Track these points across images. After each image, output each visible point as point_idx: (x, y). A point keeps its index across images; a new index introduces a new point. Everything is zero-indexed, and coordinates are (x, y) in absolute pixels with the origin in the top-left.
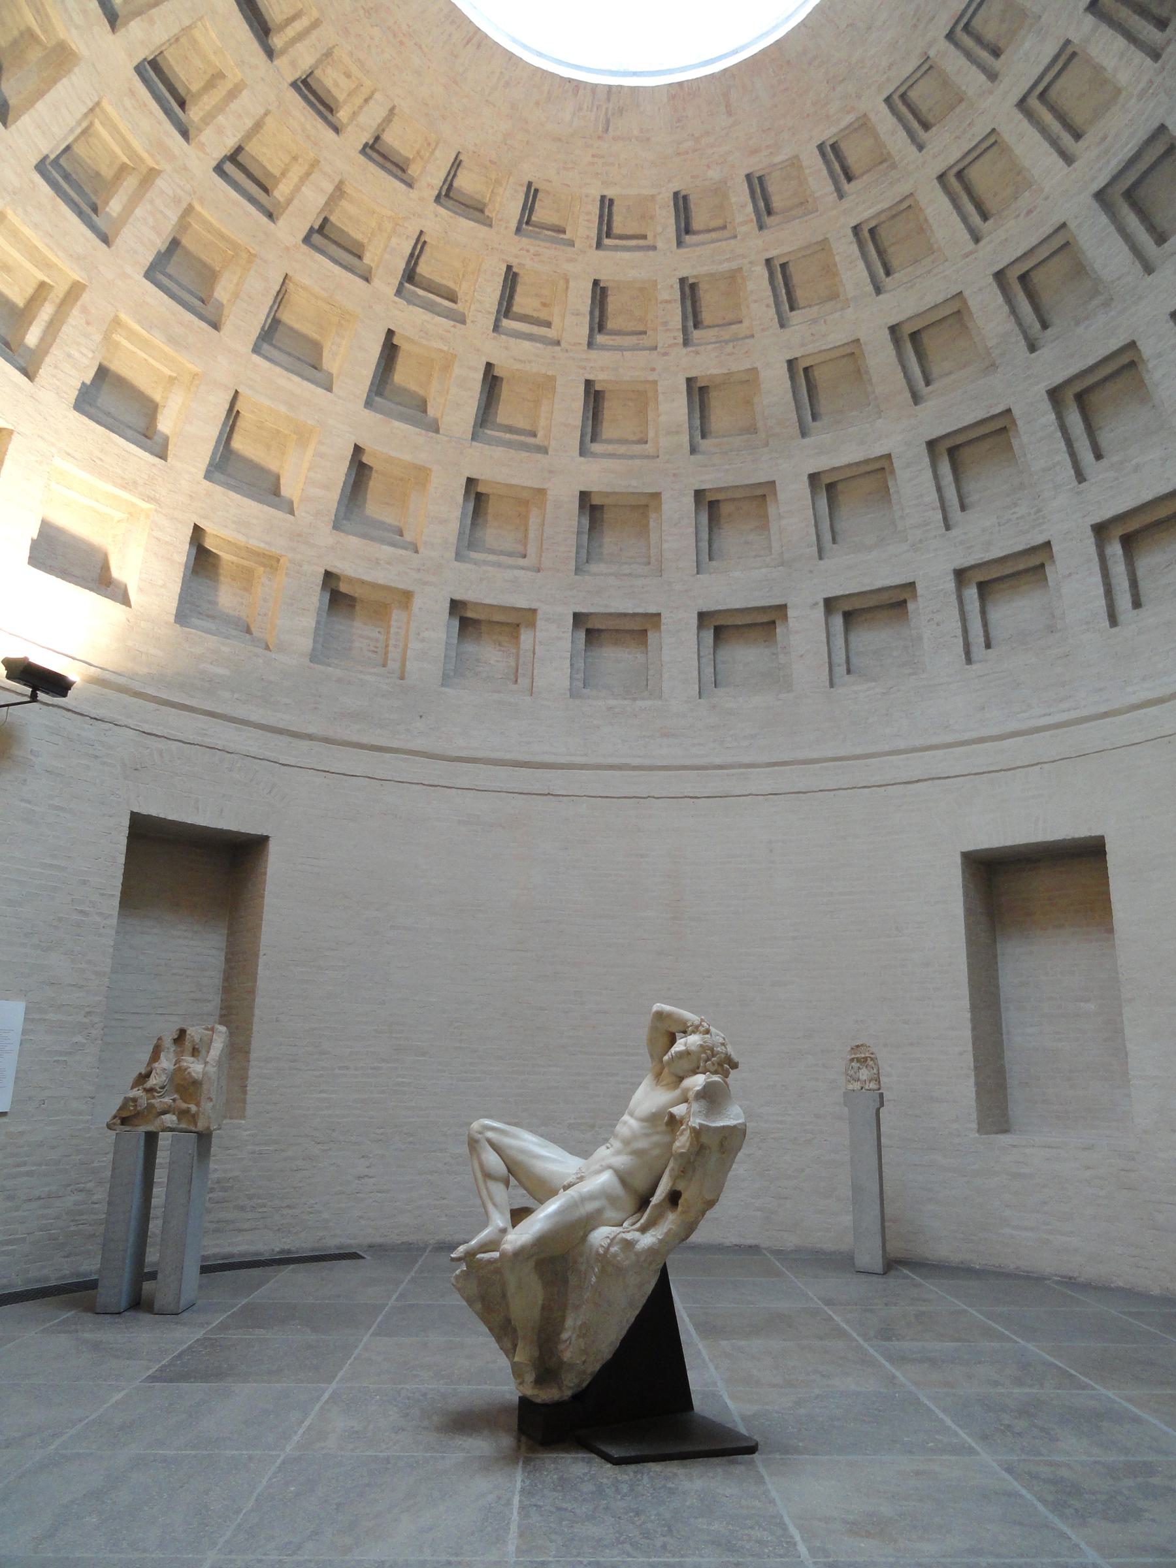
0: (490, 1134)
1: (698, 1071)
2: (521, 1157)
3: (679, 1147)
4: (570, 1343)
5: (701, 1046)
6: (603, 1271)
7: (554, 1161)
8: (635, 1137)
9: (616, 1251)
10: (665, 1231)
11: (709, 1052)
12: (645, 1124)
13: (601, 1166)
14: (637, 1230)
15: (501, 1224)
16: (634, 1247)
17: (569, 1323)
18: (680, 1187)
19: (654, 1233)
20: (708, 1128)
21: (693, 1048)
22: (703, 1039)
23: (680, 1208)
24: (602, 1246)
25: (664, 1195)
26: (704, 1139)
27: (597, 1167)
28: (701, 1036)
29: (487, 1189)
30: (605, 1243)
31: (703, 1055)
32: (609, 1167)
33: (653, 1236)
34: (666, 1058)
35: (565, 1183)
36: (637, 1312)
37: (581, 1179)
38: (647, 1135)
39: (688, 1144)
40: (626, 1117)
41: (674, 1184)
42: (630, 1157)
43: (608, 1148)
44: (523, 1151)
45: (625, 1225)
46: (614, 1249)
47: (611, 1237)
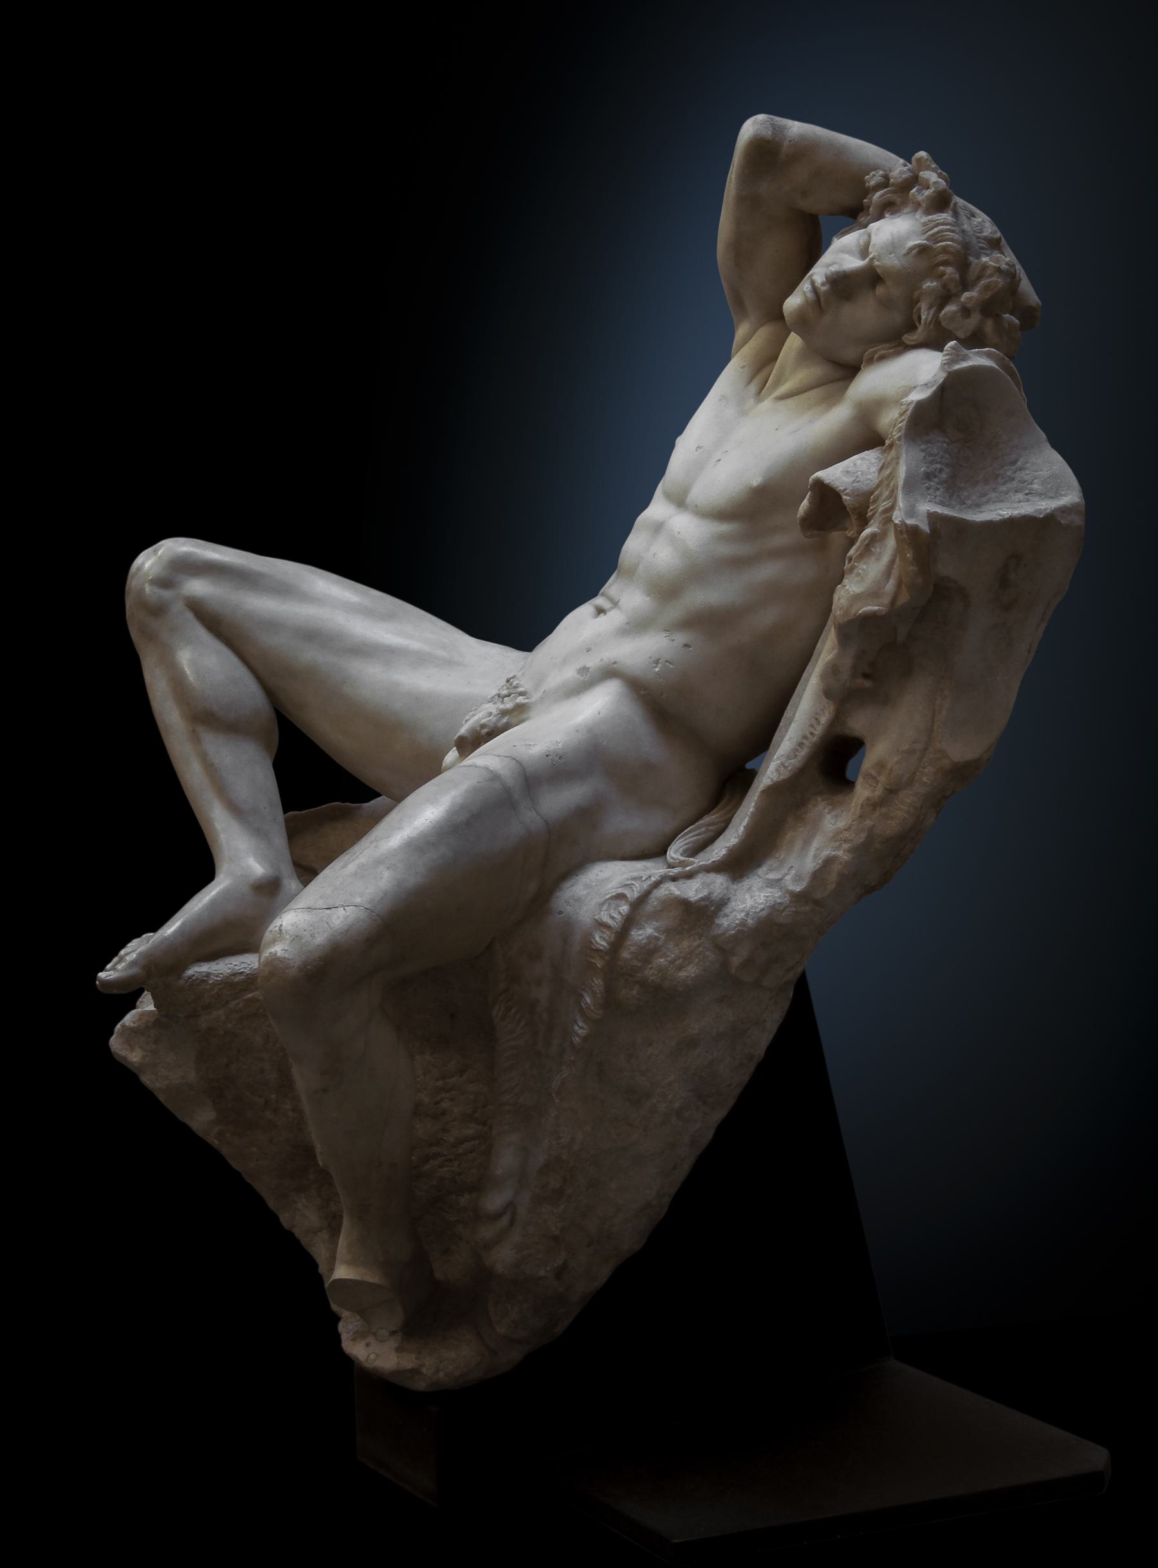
0: (198, 587)
1: (908, 338)
2: (309, 655)
3: (856, 598)
4: (512, 1222)
5: (922, 250)
6: (610, 1001)
7: (420, 660)
9: (649, 937)
11: (949, 270)
13: (584, 670)
14: (717, 868)
15: (257, 869)
16: (713, 923)
17: (505, 1160)
18: (858, 723)
19: (772, 876)
20: (960, 528)
21: (893, 261)
23: (862, 792)
24: (601, 925)
25: (803, 753)
26: (947, 567)
27: (569, 674)
28: (921, 218)
29: (204, 758)
30: (614, 915)
32: (610, 672)
33: (772, 884)
34: (793, 302)
36: (719, 1115)
38: (736, 563)
39: (890, 586)
40: (657, 509)
41: (838, 718)
42: (681, 638)
43: (600, 611)
45: (674, 852)
46: (642, 934)
47: (633, 894)
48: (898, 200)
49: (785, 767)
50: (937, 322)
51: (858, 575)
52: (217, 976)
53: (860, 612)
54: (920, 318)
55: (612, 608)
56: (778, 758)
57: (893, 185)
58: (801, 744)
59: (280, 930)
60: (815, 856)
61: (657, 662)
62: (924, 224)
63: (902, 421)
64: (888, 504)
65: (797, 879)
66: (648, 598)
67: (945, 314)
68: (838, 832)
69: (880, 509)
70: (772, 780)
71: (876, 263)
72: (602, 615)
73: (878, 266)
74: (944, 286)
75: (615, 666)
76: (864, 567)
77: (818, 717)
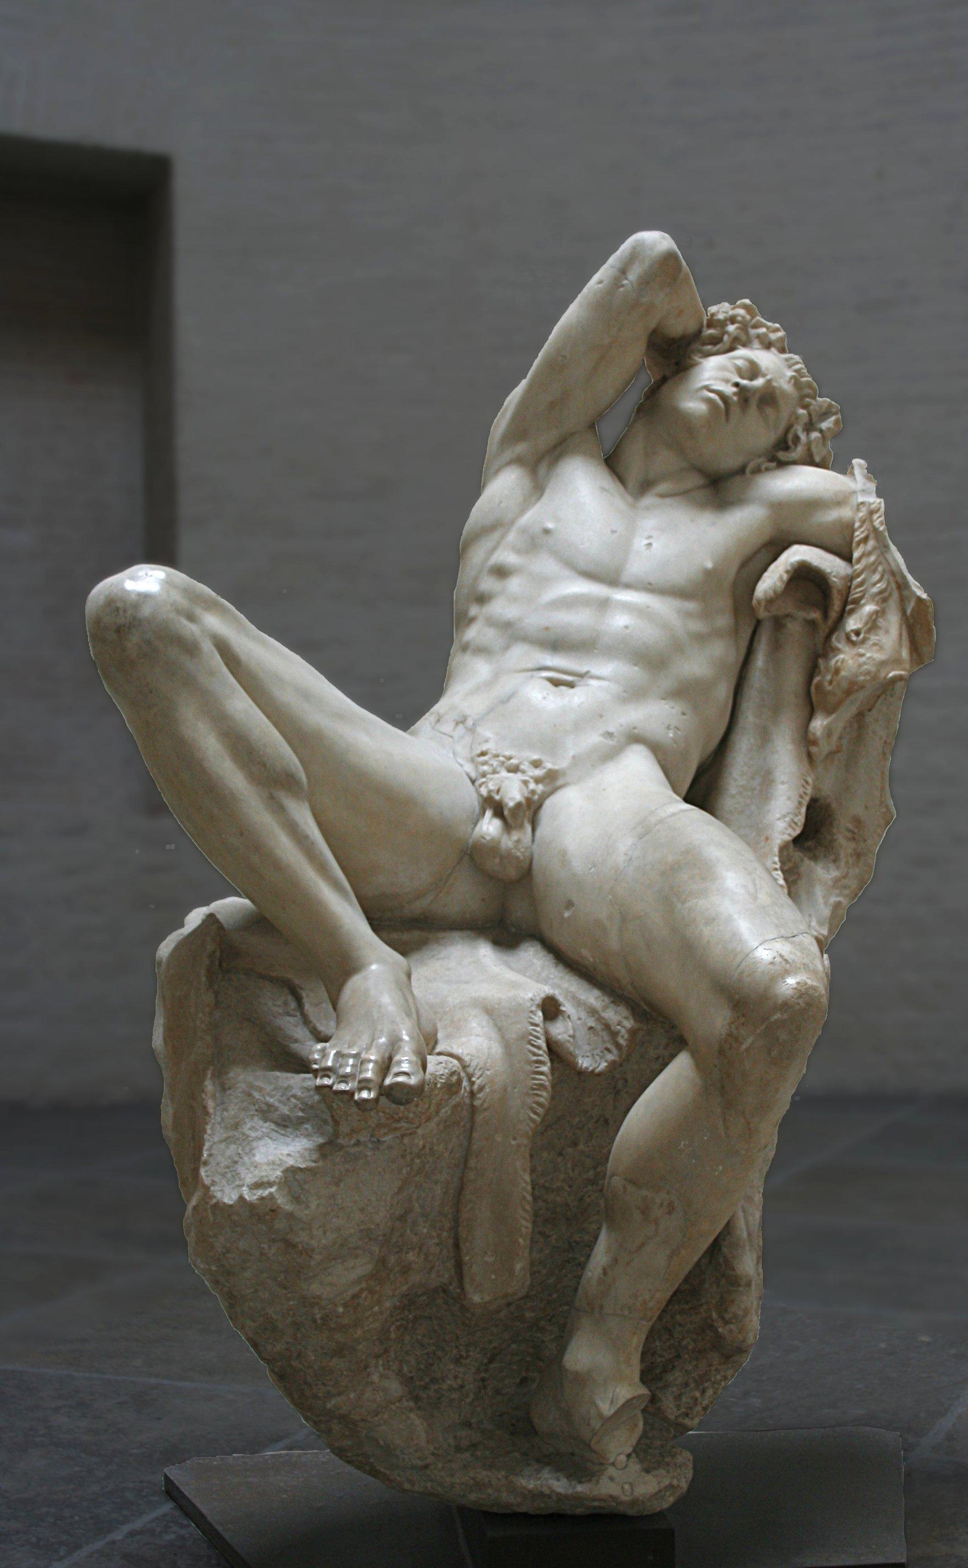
1: (782, 455)
2: (315, 718)
3: (883, 663)
8: (677, 647)
10: (827, 912)
12: (691, 606)
13: (609, 735)
25: (803, 810)
27: (593, 738)
31: (801, 411)
32: (635, 738)
37: (552, 781)
38: (701, 639)
39: (905, 654)
44: (306, 695)
48: (744, 338)
49: (796, 823)
50: (809, 444)
51: (875, 644)
52: (441, 1078)
53: (891, 675)
54: (797, 439)
55: (579, 681)
56: (784, 816)
57: (739, 322)
58: (800, 803)
59: (786, 960)
60: (826, 903)
61: (668, 728)
62: (787, 360)
63: (879, 517)
64: (883, 584)
65: (820, 923)
66: (636, 668)
67: (815, 439)
68: (836, 881)
69: (875, 590)
70: (789, 835)
71: (775, 384)
72: (563, 688)
73: (774, 388)
74: (810, 415)
75: (636, 731)
76: (877, 638)
77: (804, 777)
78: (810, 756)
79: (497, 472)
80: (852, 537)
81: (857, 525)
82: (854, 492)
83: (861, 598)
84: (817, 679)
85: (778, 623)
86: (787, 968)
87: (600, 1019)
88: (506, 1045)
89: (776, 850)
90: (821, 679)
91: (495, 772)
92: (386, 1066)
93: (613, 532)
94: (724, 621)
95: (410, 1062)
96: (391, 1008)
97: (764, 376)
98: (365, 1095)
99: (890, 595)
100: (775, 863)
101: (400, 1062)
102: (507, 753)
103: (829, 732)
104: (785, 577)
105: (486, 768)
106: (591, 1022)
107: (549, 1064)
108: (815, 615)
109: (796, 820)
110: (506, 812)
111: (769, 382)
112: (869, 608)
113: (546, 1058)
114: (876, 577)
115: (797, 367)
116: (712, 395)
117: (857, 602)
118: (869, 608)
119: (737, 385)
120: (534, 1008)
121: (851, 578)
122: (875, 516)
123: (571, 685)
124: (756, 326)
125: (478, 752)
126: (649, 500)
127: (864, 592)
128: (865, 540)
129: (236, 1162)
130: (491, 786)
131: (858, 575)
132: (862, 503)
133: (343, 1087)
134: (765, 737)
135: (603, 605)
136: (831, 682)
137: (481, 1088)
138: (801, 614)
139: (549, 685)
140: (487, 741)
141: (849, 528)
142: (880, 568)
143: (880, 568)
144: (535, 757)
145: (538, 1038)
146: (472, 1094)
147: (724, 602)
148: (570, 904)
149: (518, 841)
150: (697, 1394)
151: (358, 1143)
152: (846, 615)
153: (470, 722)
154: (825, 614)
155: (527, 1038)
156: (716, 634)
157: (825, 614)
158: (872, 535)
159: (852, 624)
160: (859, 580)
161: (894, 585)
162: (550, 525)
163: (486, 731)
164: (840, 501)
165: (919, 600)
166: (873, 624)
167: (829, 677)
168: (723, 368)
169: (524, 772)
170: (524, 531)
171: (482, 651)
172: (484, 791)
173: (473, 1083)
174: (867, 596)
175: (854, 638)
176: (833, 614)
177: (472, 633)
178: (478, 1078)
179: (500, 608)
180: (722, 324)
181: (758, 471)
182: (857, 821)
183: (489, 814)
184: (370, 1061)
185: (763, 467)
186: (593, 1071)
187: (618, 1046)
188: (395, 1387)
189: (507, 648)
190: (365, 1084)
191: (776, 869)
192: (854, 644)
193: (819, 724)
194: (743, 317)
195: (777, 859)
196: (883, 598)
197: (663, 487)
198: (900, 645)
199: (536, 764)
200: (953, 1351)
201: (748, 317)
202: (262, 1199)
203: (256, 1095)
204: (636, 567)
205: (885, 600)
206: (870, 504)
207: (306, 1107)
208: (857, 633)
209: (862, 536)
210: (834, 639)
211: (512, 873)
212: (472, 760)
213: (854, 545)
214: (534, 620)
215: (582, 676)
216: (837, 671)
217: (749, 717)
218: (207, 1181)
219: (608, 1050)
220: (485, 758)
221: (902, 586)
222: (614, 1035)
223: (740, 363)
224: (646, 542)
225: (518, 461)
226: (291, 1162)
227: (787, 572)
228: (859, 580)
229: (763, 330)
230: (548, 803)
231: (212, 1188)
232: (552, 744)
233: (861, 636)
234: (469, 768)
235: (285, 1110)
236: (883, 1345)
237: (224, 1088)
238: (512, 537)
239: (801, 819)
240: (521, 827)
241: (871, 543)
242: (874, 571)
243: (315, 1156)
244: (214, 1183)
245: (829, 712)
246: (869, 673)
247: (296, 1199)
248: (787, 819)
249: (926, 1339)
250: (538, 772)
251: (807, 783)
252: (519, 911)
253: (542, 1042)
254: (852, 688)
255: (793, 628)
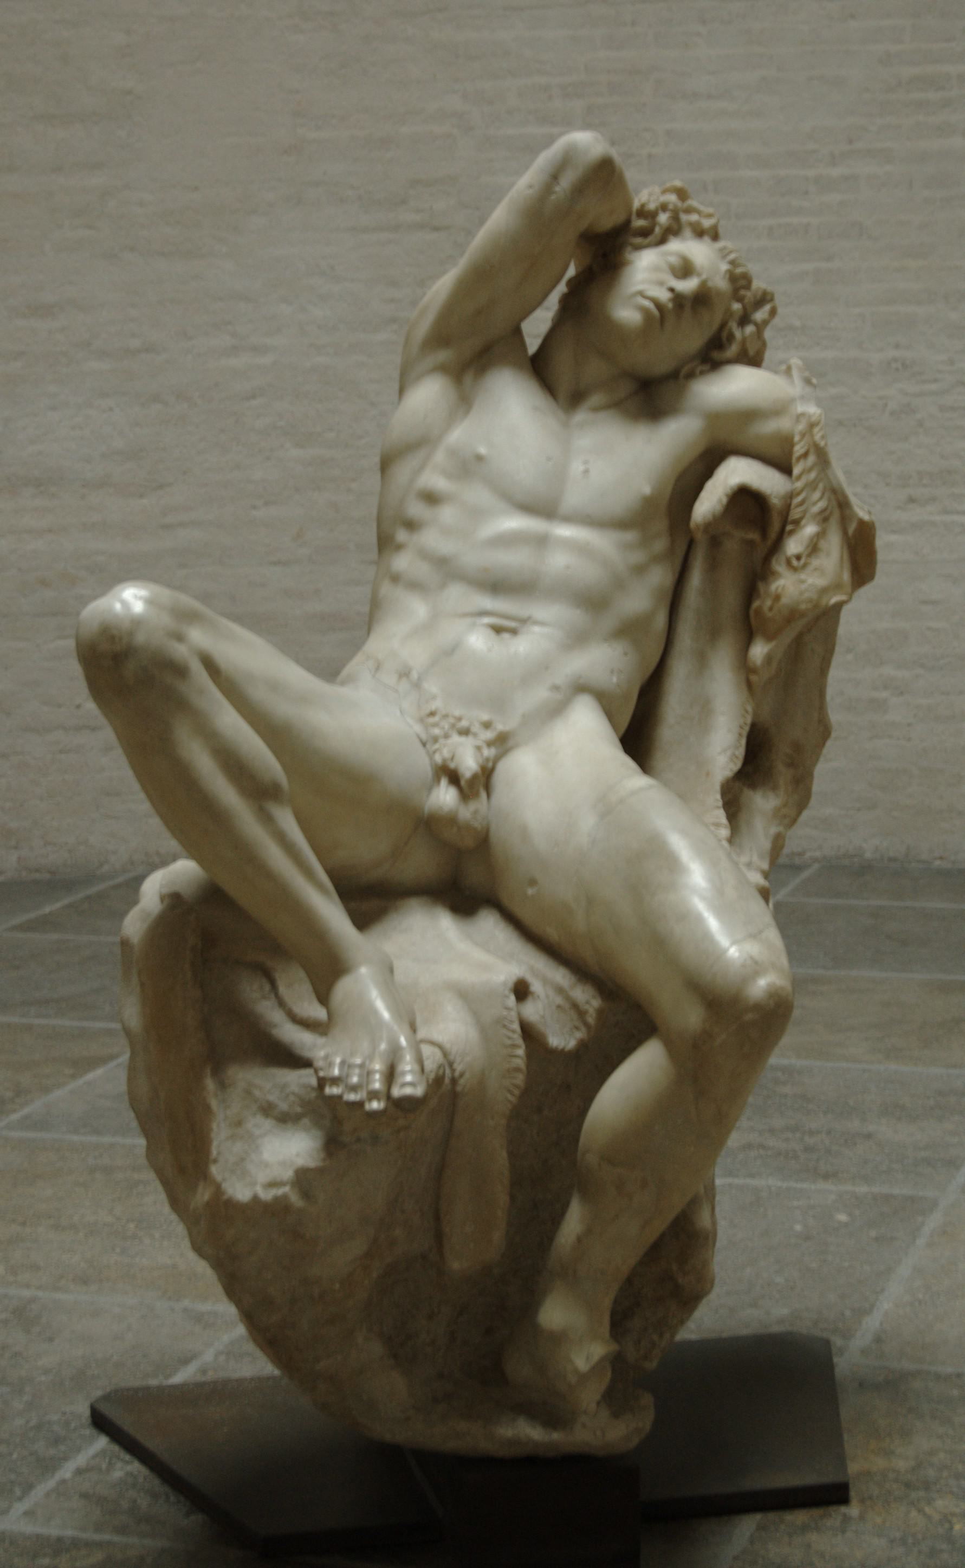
0: (198, 636)
1: (716, 355)
2: (282, 709)
3: (824, 591)
8: (618, 584)
10: (766, 845)
12: (630, 536)
13: (556, 688)
21: (721, 283)
22: (723, 253)
25: (744, 742)
27: (540, 694)
31: (737, 306)
32: (580, 688)
35: (469, 763)
37: (503, 743)
38: (639, 570)
39: (846, 576)
44: (275, 686)
48: (675, 227)
49: (737, 757)
51: (815, 569)
54: (731, 337)
57: (672, 211)
58: (740, 735)
61: (612, 672)
62: (721, 250)
63: (819, 431)
66: (578, 612)
69: (816, 509)
71: (710, 284)
72: (506, 636)
74: (744, 307)
78: (749, 685)
79: (419, 378)
80: (790, 453)
81: (796, 439)
82: (793, 400)
83: (801, 518)
84: (756, 604)
85: (715, 542)
86: (757, 968)
87: (568, 998)
88: (483, 1030)
89: (718, 787)
90: (763, 604)
91: (446, 736)
92: (391, 1075)
93: (549, 459)
94: (660, 545)
95: (411, 1071)
96: (386, 1015)
97: (699, 275)
98: (375, 1105)
99: (831, 513)
100: (717, 800)
101: (404, 1073)
102: (457, 713)
103: (769, 659)
104: (725, 500)
105: (437, 731)
106: (559, 1000)
107: (523, 1047)
108: (754, 536)
109: (737, 753)
110: (463, 783)
111: (703, 284)
112: (810, 529)
113: (520, 1041)
114: (817, 495)
115: (732, 256)
116: (647, 304)
117: (797, 522)
118: (810, 529)
119: (672, 290)
120: (507, 992)
121: (791, 496)
122: (816, 430)
123: (514, 632)
124: (689, 211)
125: (428, 711)
126: (581, 416)
127: (805, 512)
128: (805, 455)
129: (243, 1160)
130: (446, 753)
131: (798, 494)
132: (803, 414)
133: (352, 1097)
134: (702, 660)
135: (541, 542)
136: (771, 609)
137: (462, 1075)
138: (739, 534)
139: (492, 634)
140: (434, 697)
141: (787, 442)
142: (821, 486)
143: (821, 486)
144: (485, 717)
145: (512, 1022)
146: (454, 1081)
147: (661, 525)
148: (533, 882)
149: (476, 812)
150: (655, 1337)
151: (358, 1140)
152: (786, 535)
153: (415, 675)
154: (764, 532)
155: (501, 1022)
156: (656, 559)
157: (764, 532)
158: (812, 451)
159: (793, 546)
160: (799, 499)
161: (834, 503)
162: (482, 450)
163: (432, 687)
164: (778, 410)
165: (861, 523)
166: (814, 548)
167: (768, 603)
168: (656, 269)
169: (475, 735)
170: (453, 453)
171: (416, 586)
172: (438, 758)
173: (453, 1071)
174: (808, 515)
175: (795, 563)
176: (773, 534)
177: (402, 562)
178: (460, 1063)
179: (430, 539)
180: (652, 215)
181: (691, 375)
182: (797, 747)
183: (444, 782)
184: (376, 1071)
185: (698, 371)
186: (563, 1050)
187: (586, 1024)
188: (377, 1349)
189: (443, 586)
190: (373, 1095)
191: (718, 807)
192: (795, 569)
193: (759, 651)
194: (675, 206)
195: (719, 796)
196: (824, 518)
197: (596, 399)
198: (842, 567)
199: (487, 725)
200: (873, 1233)
201: (679, 204)
202: (276, 1199)
203: (257, 1093)
204: (573, 498)
205: (826, 520)
206: (810, 416)
207: (304, 1103)
208: (798, 557)
209: (802, 451)
210: (774, 562)
211: (469, 842)
212: (421, 721)
213: (794, 460)
214: (472, 559)
215: (525, 621)
216: (777, 598)
217: (685, 639)
218: (219, 1178)
219: (577, 1028)
220: (436, 719)
221: (843, 504)
222: (581, 1014)
223: (673, 260)
224: (581, 468)
225: (443, 369)
226: (301, 1162)
227: (727, 495)
228: (799, 499)
229: (694, 217)
230: (501, 767)
231: (224, 1185)
232: (499, 702)
233: (802, 561)
234: (418, 728)
235: (284, 1106)
236: (798, 1228)
237: (223, 1085)
238: (440, 456)
239: (741, 752)
240: (476, 795)
241: (811, 459)
242: (815, 489)
243: (322, 1155)
244: (224, 1180)
245: (769, 637)
246: (810, 601)
247: (306, 1194)
248: (729, 753)
249: (842, 1217)
250: (489, 735)
251: (747, 712)
252: (474, 876)
253: (516, 1026)
254: (793, 615)
255: (732, 546)
